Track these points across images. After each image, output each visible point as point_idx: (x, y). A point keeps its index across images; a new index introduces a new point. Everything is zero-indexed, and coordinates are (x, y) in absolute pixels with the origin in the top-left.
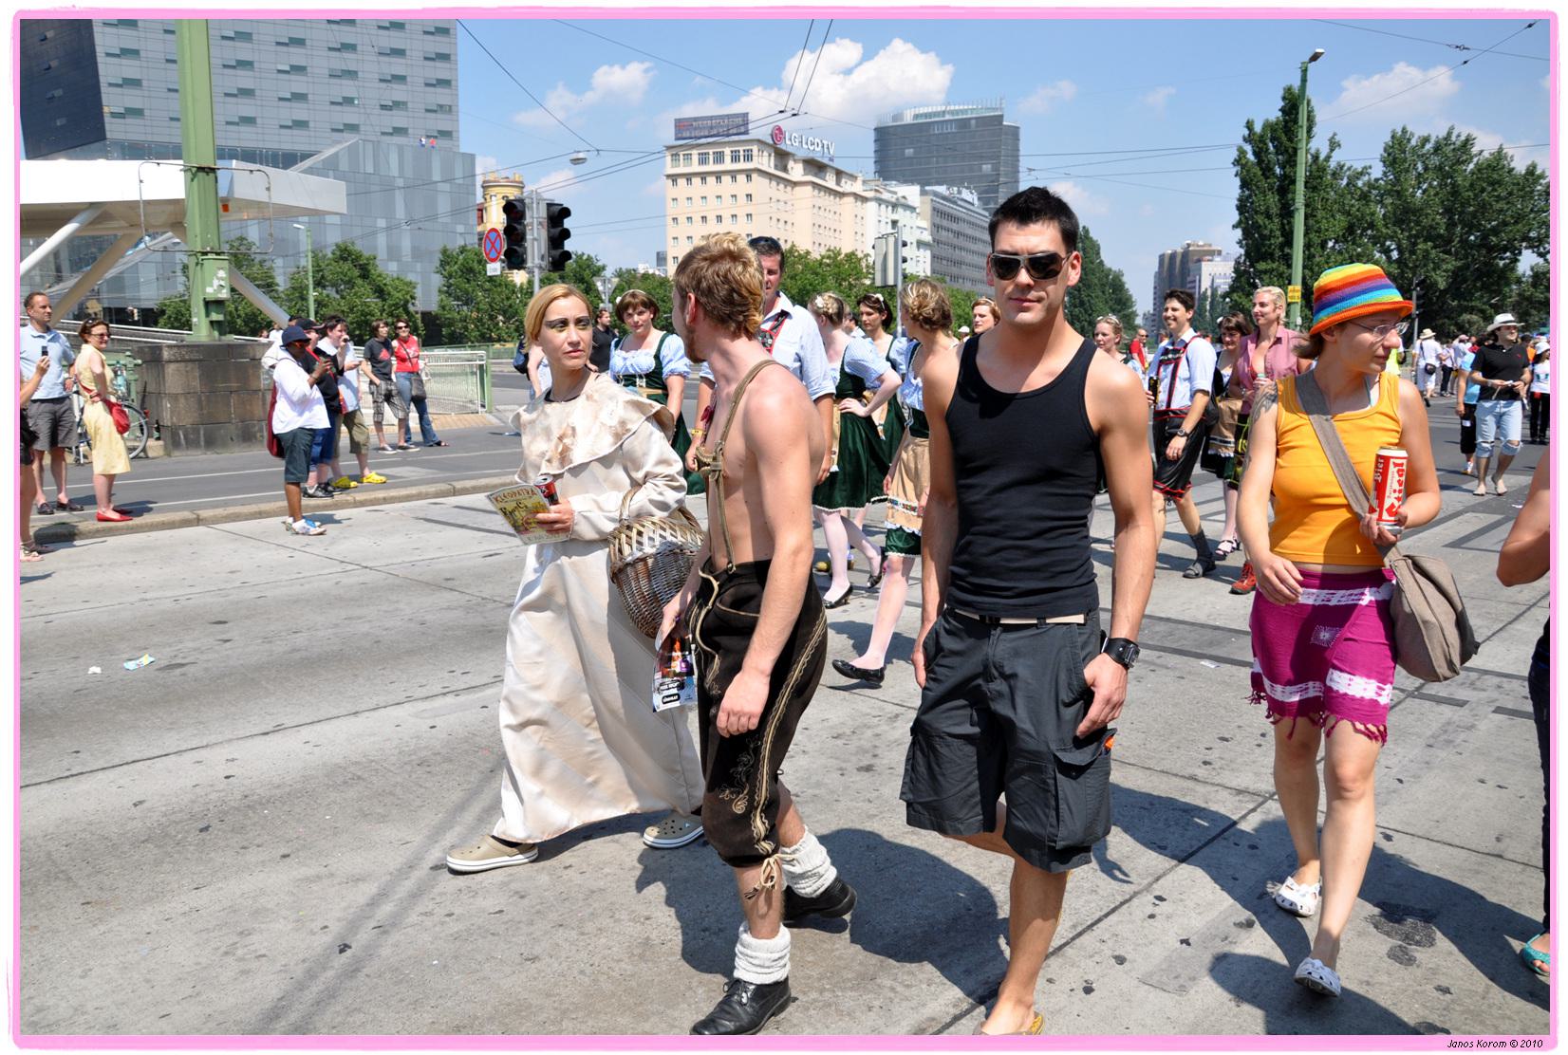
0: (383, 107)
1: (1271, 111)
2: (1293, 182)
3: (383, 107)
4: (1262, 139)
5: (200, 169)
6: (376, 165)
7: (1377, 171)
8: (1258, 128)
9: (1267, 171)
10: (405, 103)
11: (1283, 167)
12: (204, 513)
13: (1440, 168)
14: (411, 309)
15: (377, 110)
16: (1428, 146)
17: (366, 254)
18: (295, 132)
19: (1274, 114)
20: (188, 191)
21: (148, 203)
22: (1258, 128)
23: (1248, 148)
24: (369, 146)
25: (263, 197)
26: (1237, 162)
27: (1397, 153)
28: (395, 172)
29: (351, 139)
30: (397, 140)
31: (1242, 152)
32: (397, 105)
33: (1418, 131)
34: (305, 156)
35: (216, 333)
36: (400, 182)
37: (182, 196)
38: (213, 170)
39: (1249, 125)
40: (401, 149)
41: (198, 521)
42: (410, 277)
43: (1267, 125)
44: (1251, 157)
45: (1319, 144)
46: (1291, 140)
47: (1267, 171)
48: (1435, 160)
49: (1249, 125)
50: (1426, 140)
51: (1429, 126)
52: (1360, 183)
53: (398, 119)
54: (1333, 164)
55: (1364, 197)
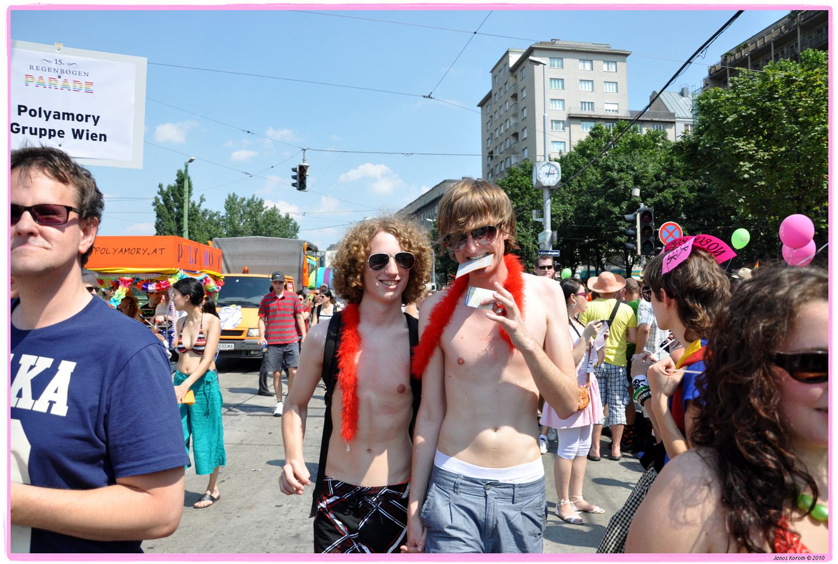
1: (171, 181)
2: (182, 216)
4: (167, 194)
7: (223, 212)
8: (165, 189)
9: (170, 209)
11: (178, 208)
13: (250, 213)
16: (245, 202)
19: (173, 182)
22: (165, 189)
23: (160, 197)
26: (154, 204)
27: (231, 204)
31: (157, 200)
33: (240, 195)
39: (160, 186)
43: (169, 187)
44: (162, 202)
45: (195, 198)
46: (181, 196)
47: (170, 209)
48: (248, 209)
49: (160, 186)
50: (243, 199)
51: (244, 193)
52: (215, 218)
54: (202, 208)
55: (217, 225)
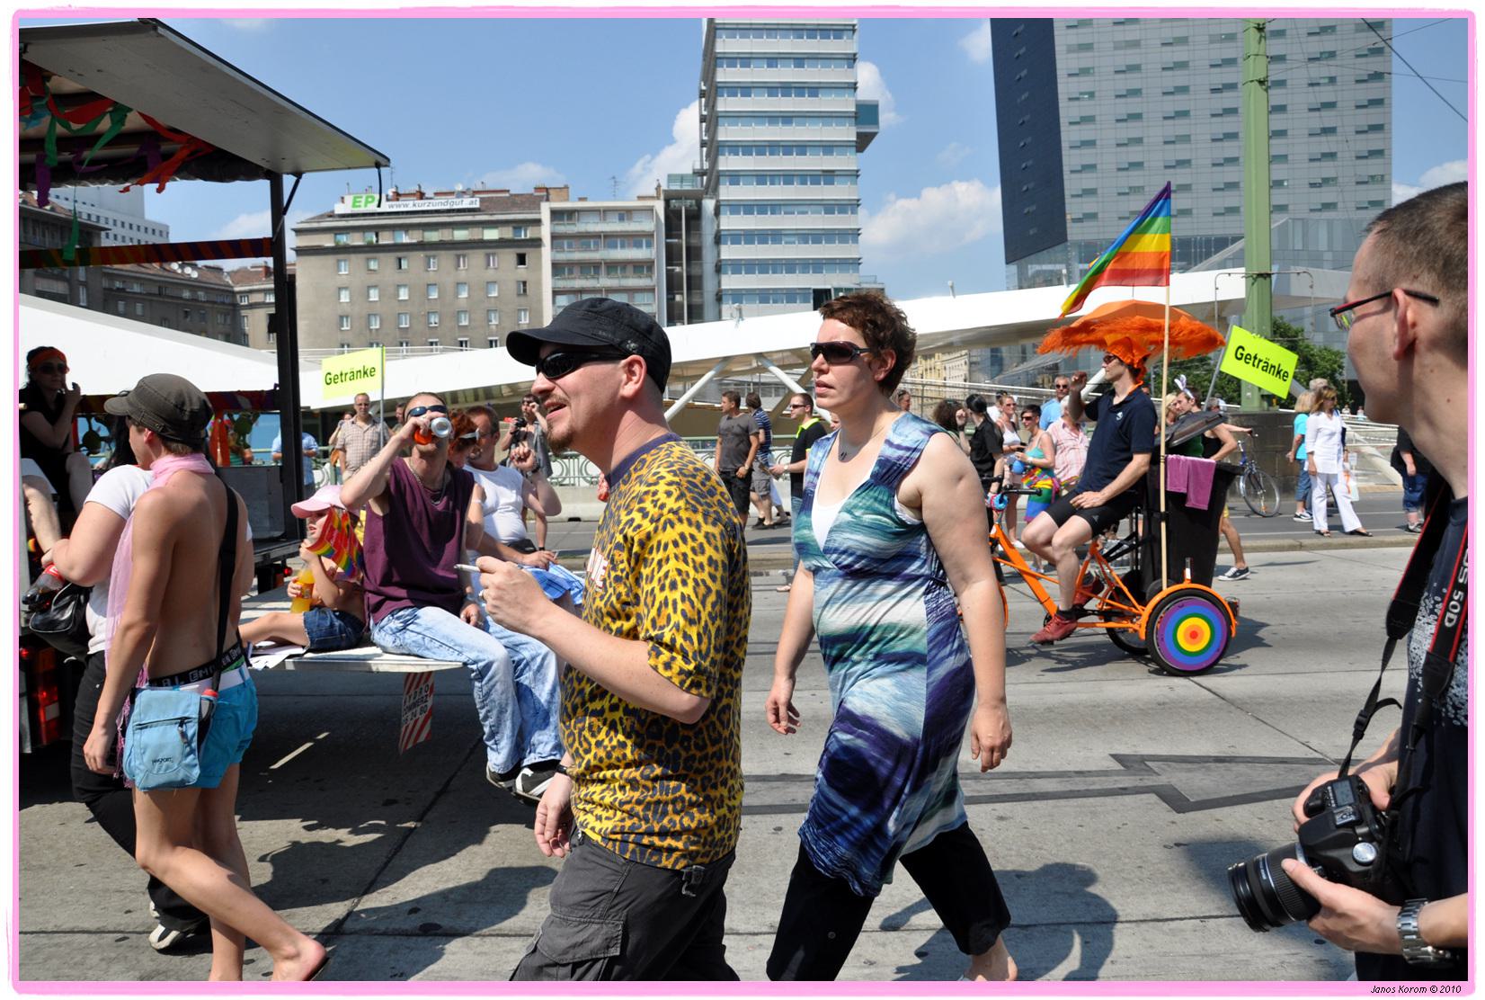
0: (1312, 185)
3: (1312, 185)
5: (1260, 275)
6: (1305, 244)
10: (1334, 179)
12: (1306, 542)
14: (1338, 377)
15: (1307, 189)
17: (1295, 326)
18: (1227, 218)
20: (1248, 292)
21: (1220, 303)
24: (1299, 224)
25: (1307, 293)
28: (1323, 245)
29: (1280, 219)
30: (1326, 215)
32: (1326, 181)
34: (1235, 239)
35: (1265, 404)
36: (1328, 256)
37: (1242, 295)
38: (1269, 275)
40: (1330, 223)
41: (1301, 547)
42: (1336, 347)
53: (1328, 195)
